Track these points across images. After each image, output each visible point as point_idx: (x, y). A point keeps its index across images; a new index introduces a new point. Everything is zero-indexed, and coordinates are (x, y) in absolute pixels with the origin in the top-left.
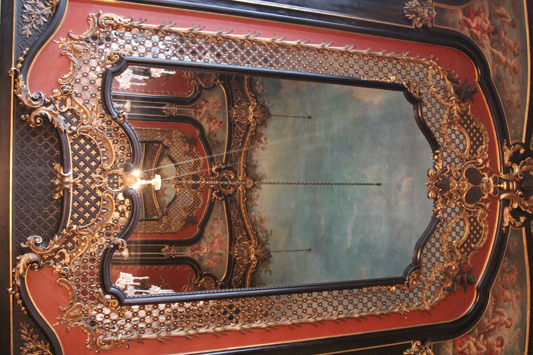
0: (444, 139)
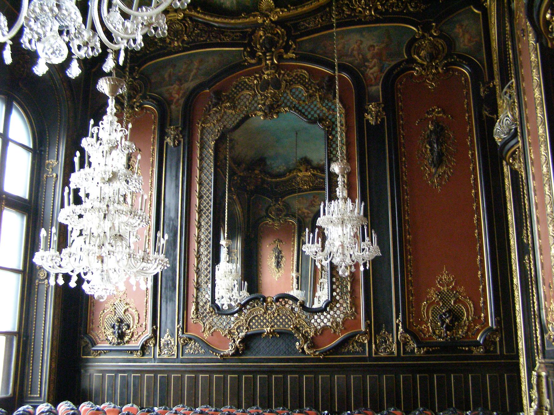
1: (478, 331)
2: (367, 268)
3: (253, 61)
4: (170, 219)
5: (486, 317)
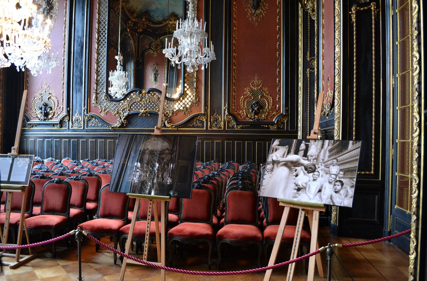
1: (274, 115)
2: (206, 67)
4: (78, 37)
5: (279, 107)
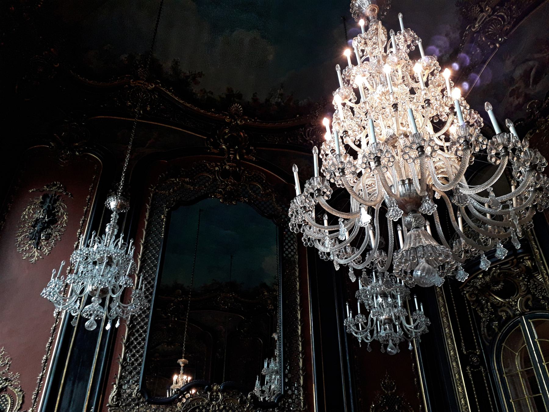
0: (202, 189)
3: (215, 151)
